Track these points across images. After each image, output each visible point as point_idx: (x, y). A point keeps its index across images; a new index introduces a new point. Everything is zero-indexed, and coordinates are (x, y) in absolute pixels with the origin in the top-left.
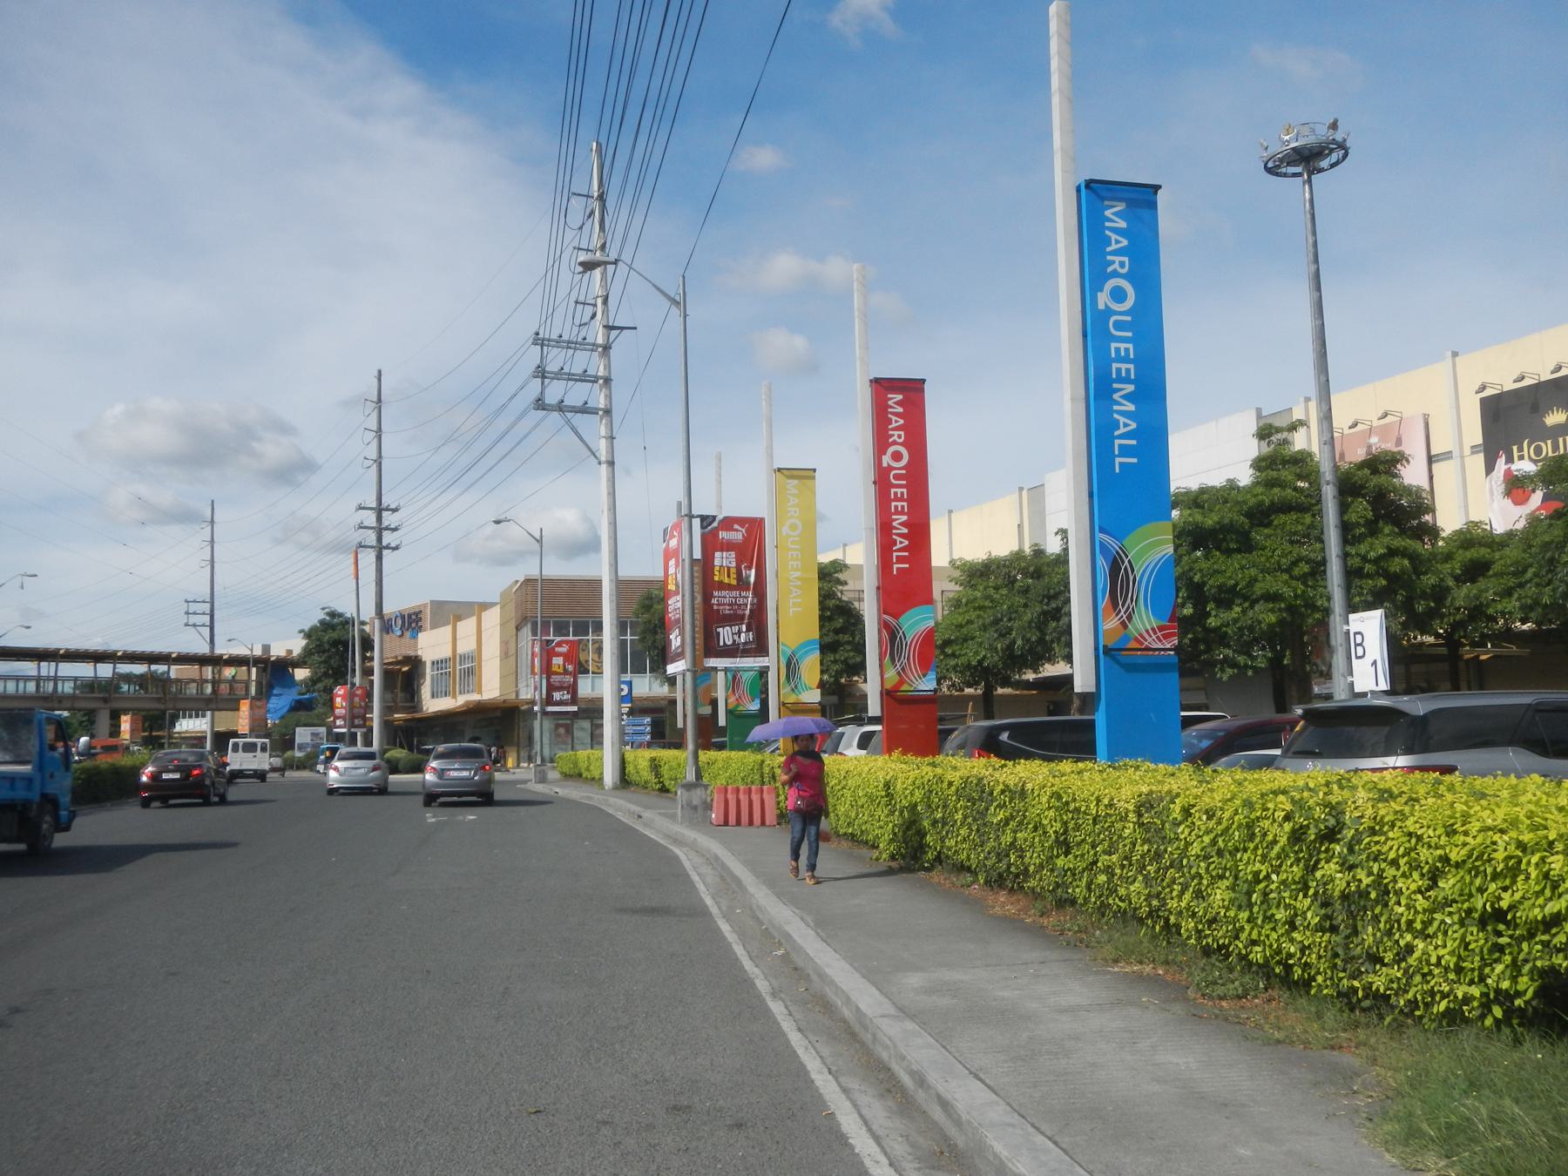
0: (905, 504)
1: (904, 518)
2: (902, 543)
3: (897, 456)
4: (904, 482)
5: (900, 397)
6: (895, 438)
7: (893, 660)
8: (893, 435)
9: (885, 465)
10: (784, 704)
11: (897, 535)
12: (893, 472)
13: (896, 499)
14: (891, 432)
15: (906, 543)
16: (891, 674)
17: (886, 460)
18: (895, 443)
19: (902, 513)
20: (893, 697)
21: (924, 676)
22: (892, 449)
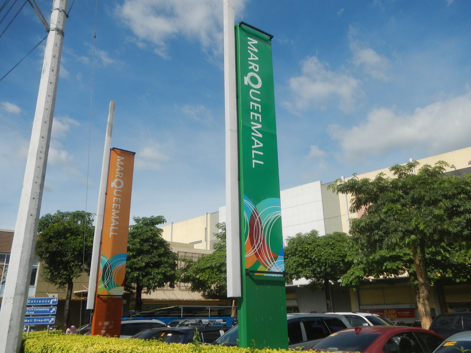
0: (260, 116)
1: (260, 126)
2: (258, 144)
3: (254, 80)
4: (259, 100)
5: (256, 42)
6: (253, 67)
7: (252, 242)
8: (252, 65)
9: (246, 83)
10: (99, 296)
11: (254, 137)
12: (251, 91)
13: (254, 110)
14: (249, 62)
15: (261, 145)
16: (250, 254)
17: (247, 80)
18: (252, 70)
19: (257, 121)
20: (251, 277)
21: (276, 258)
22: (250, 74)
